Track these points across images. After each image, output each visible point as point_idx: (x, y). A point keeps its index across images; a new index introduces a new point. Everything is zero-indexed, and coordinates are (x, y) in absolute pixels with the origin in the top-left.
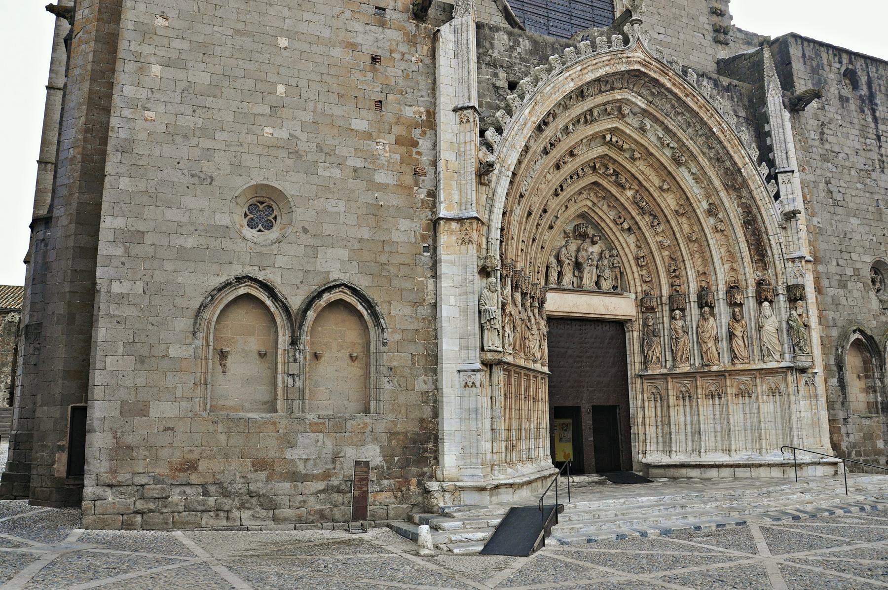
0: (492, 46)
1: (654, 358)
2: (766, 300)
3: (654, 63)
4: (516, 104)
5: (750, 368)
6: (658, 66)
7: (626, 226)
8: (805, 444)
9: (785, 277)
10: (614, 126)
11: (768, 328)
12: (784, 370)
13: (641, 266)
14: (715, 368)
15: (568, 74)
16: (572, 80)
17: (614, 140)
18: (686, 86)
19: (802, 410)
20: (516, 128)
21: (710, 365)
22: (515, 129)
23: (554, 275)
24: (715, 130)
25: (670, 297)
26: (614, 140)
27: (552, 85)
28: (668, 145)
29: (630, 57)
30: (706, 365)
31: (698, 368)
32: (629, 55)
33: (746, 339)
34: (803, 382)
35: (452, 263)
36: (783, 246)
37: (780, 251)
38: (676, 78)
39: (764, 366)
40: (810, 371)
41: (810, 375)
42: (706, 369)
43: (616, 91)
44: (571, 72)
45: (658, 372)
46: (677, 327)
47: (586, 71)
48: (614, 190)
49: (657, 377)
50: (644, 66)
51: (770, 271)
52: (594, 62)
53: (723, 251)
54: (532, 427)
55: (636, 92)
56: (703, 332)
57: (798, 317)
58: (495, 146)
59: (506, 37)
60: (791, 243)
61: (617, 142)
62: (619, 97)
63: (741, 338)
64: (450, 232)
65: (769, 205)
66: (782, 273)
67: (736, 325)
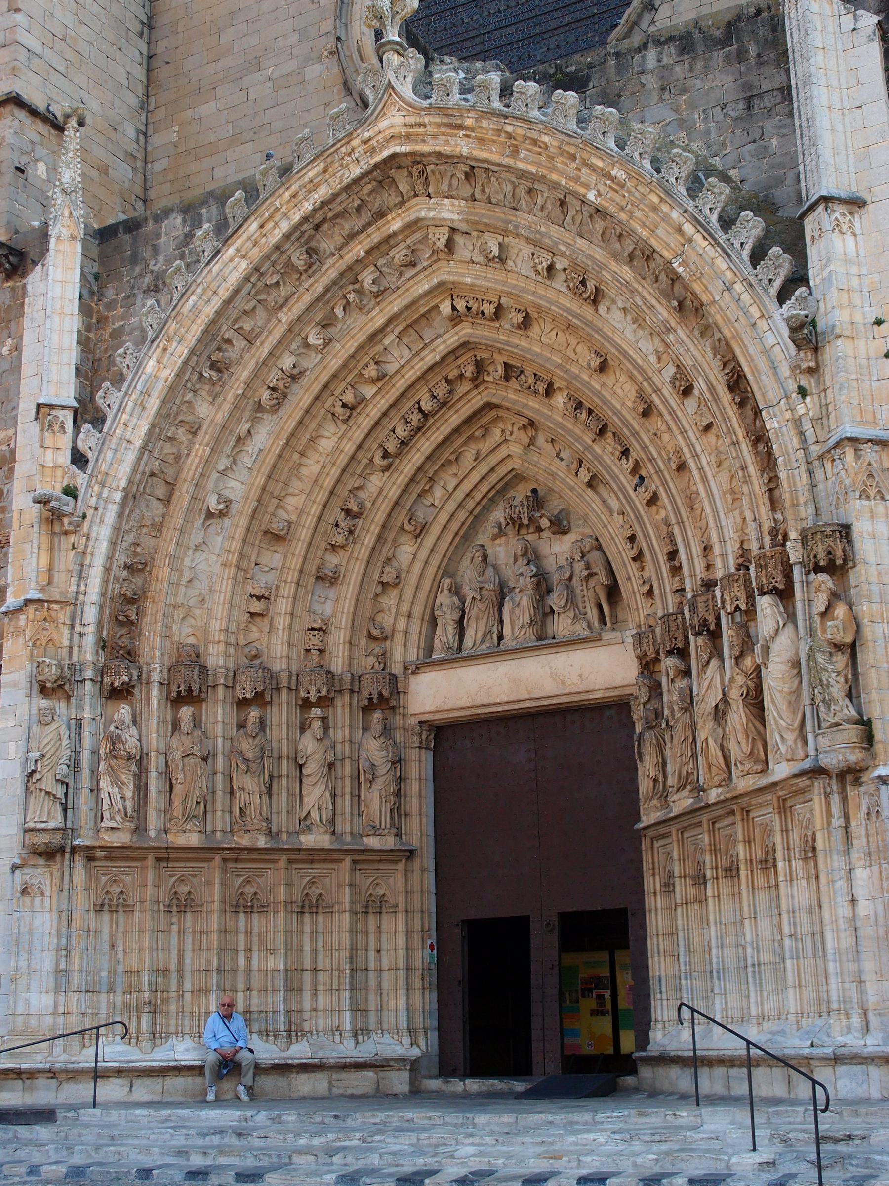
0: (156, 250)
3: (426, 120)
4: (127, 361)
6: (437, 120)
7: (584, 476)
8: (872, 999)
9: (811, 510)
10: (435, 281)
12: (803, 782)
13: (634, 559)
14: (713, 795)
15: (231, 251)
16: (243, 257)
17: (461, 306)
18: (509, 129)
19: (861, 893)
20: (130, 404)
22: (128, 409)
23: (446, 634)
24: (591, 196)
26: (461, 306)
27: (199, 290)
28: (550, 268)
29: (370, 139)
32: (367, 135)
34: (864, 809)
35: (15, 685)
36: (807, 426)
37: (796, 443)
38: (485, 123)
40: (865, 778)
41: (871, 788)
43: (390, 217)
44: (239, 241)
47: (271, 225)
48: (533, 405)
50: (408, 137)
52: (287, 195)
53: (724, 476)
54: (282, 967)
55: (438, 194)
58: (89, 455)
59: (179, 220)
60: (831, 408)
61: (469, 309)
62: (396, 226)
64: (19, 632)
65: (762, 325)
66: (806, 503)
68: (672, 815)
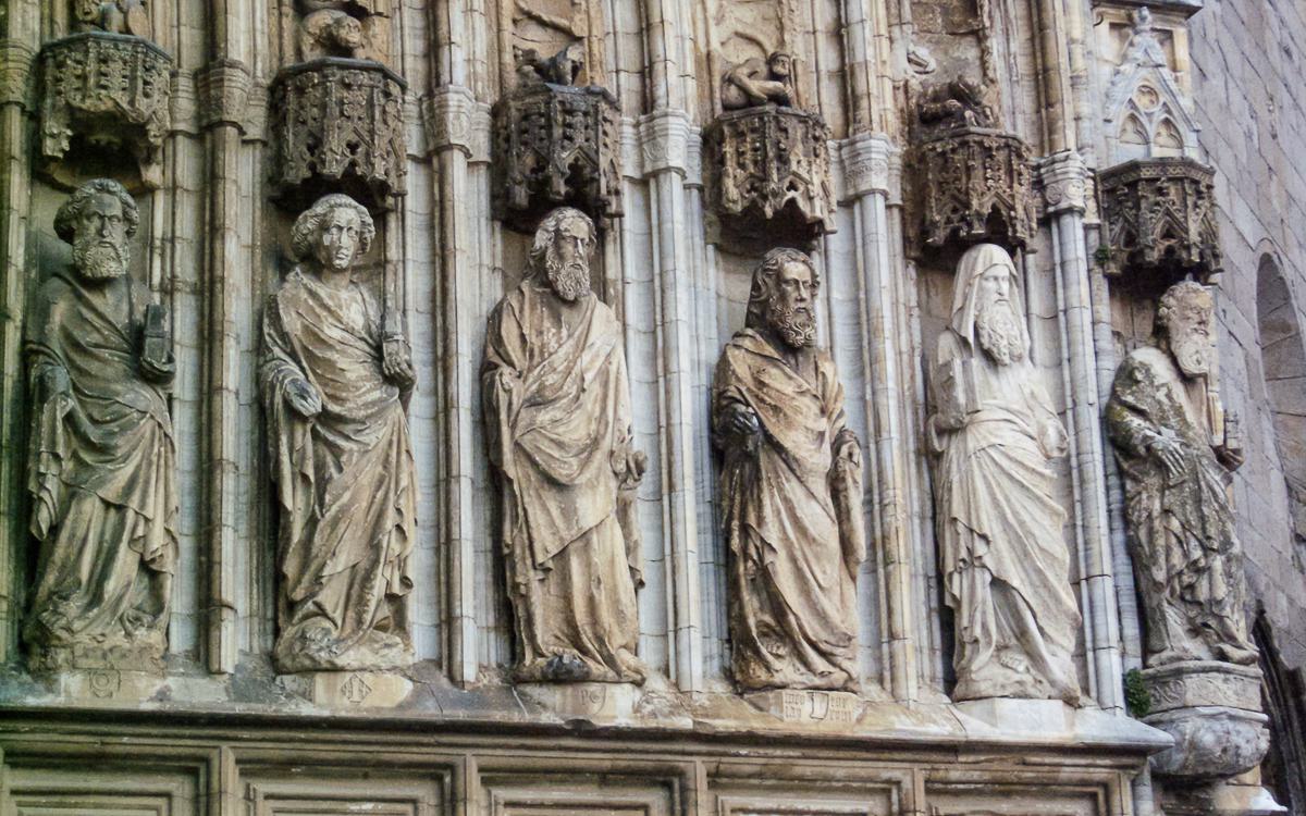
1: (126, 563)
2: (1000, 230)
5: (871, 730)
11: (1008, 436)
12: (1100, 770)
14: (617, 707)
21: (585, 678)
25: (282, 90)
30: (559, 676)
31: (478, 697)
33: (856, 499)
39: (973, 725)
42: (553, 706)
45: (142, 692)
46: (332, 333)
49: (126, 742)
51: (995, 43)
56: (537, 402)
57: (1179, 391)
63: (821, 488)
67: (776, 378)
68: (306, 710)
